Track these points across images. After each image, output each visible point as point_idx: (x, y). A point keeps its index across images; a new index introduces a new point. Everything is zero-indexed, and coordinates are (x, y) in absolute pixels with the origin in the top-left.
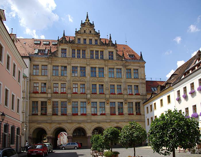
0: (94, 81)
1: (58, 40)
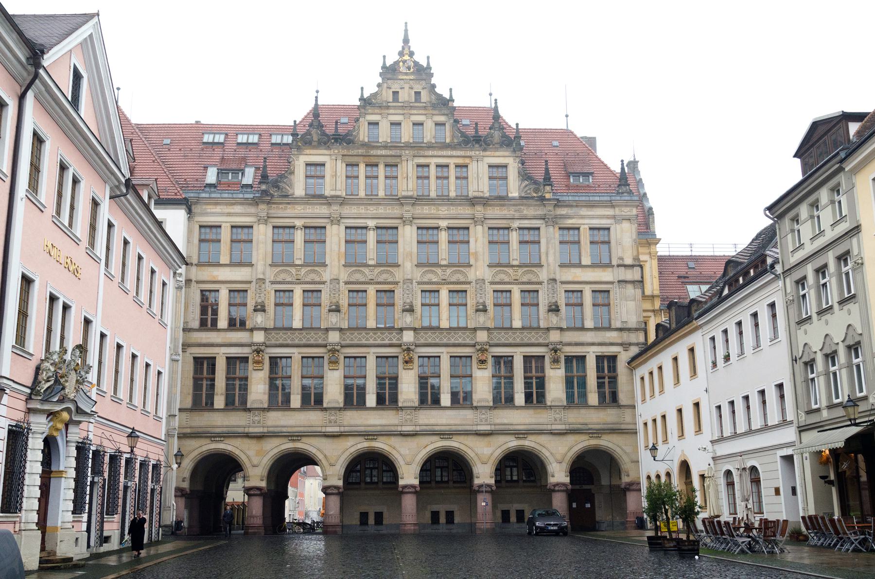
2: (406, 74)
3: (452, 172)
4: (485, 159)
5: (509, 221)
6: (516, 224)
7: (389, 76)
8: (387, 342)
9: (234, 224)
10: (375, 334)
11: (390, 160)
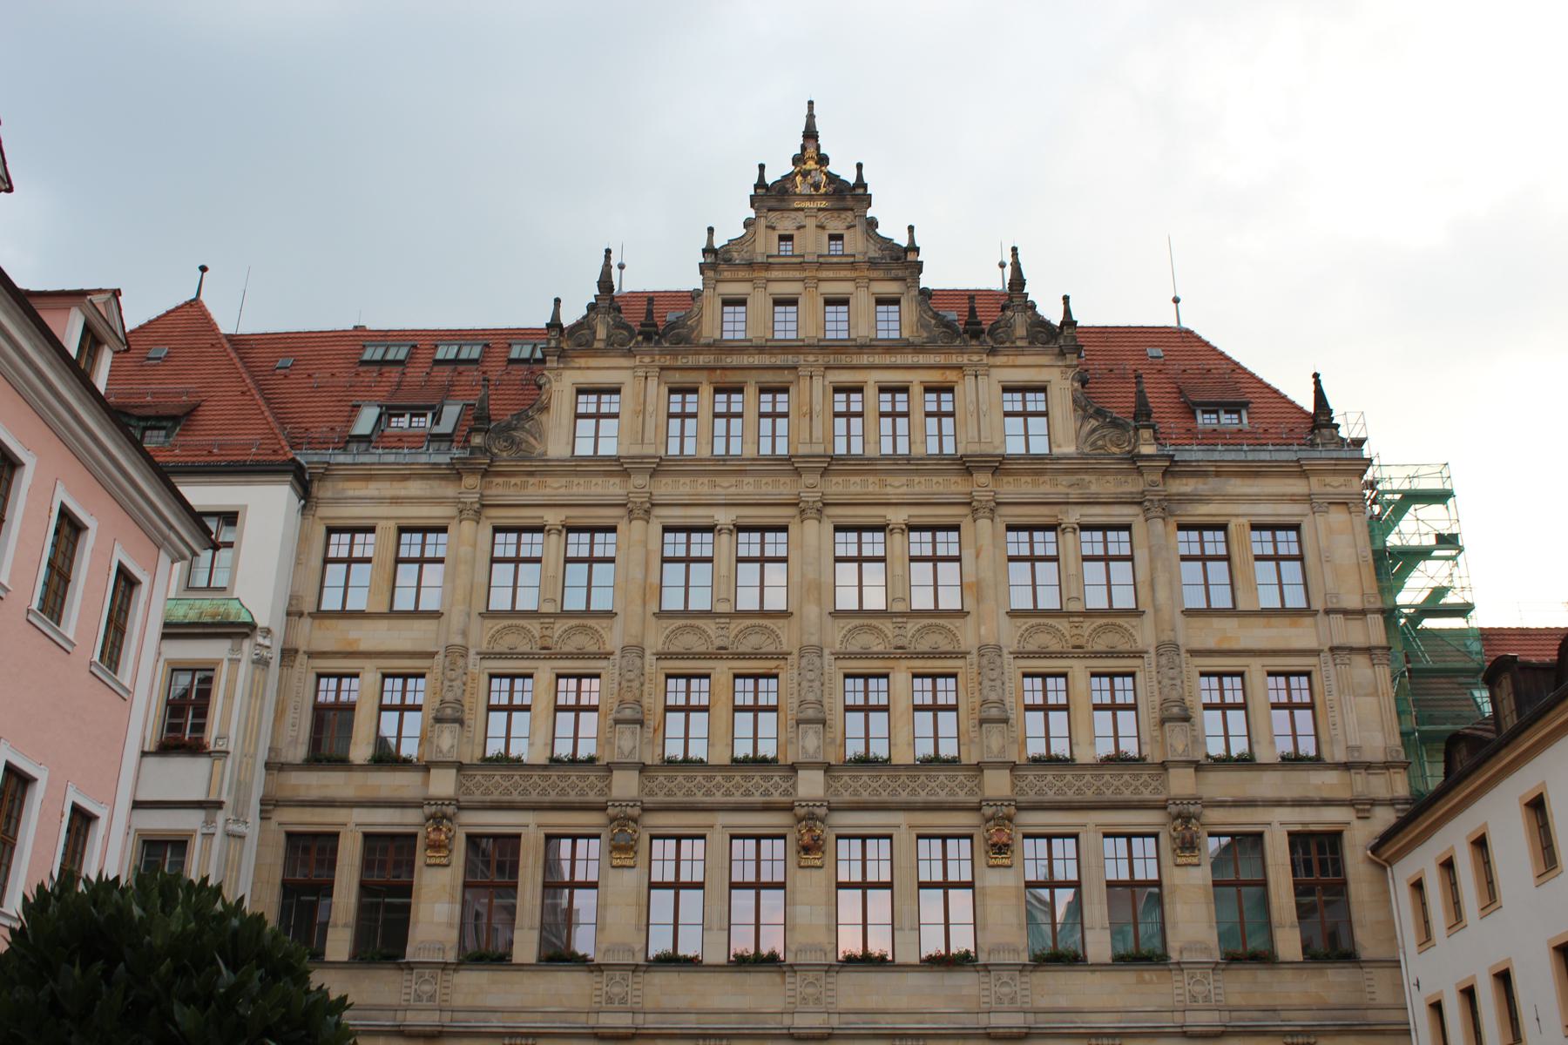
0: (866, 655)
1: (555, 324)
4: (993, 371)
5: (1056, 509)
6: (1073, 516)
7: (773, 203)
8: (757, 798)
9: (405, 523)
10: (728, 779)
11: (770, 378)
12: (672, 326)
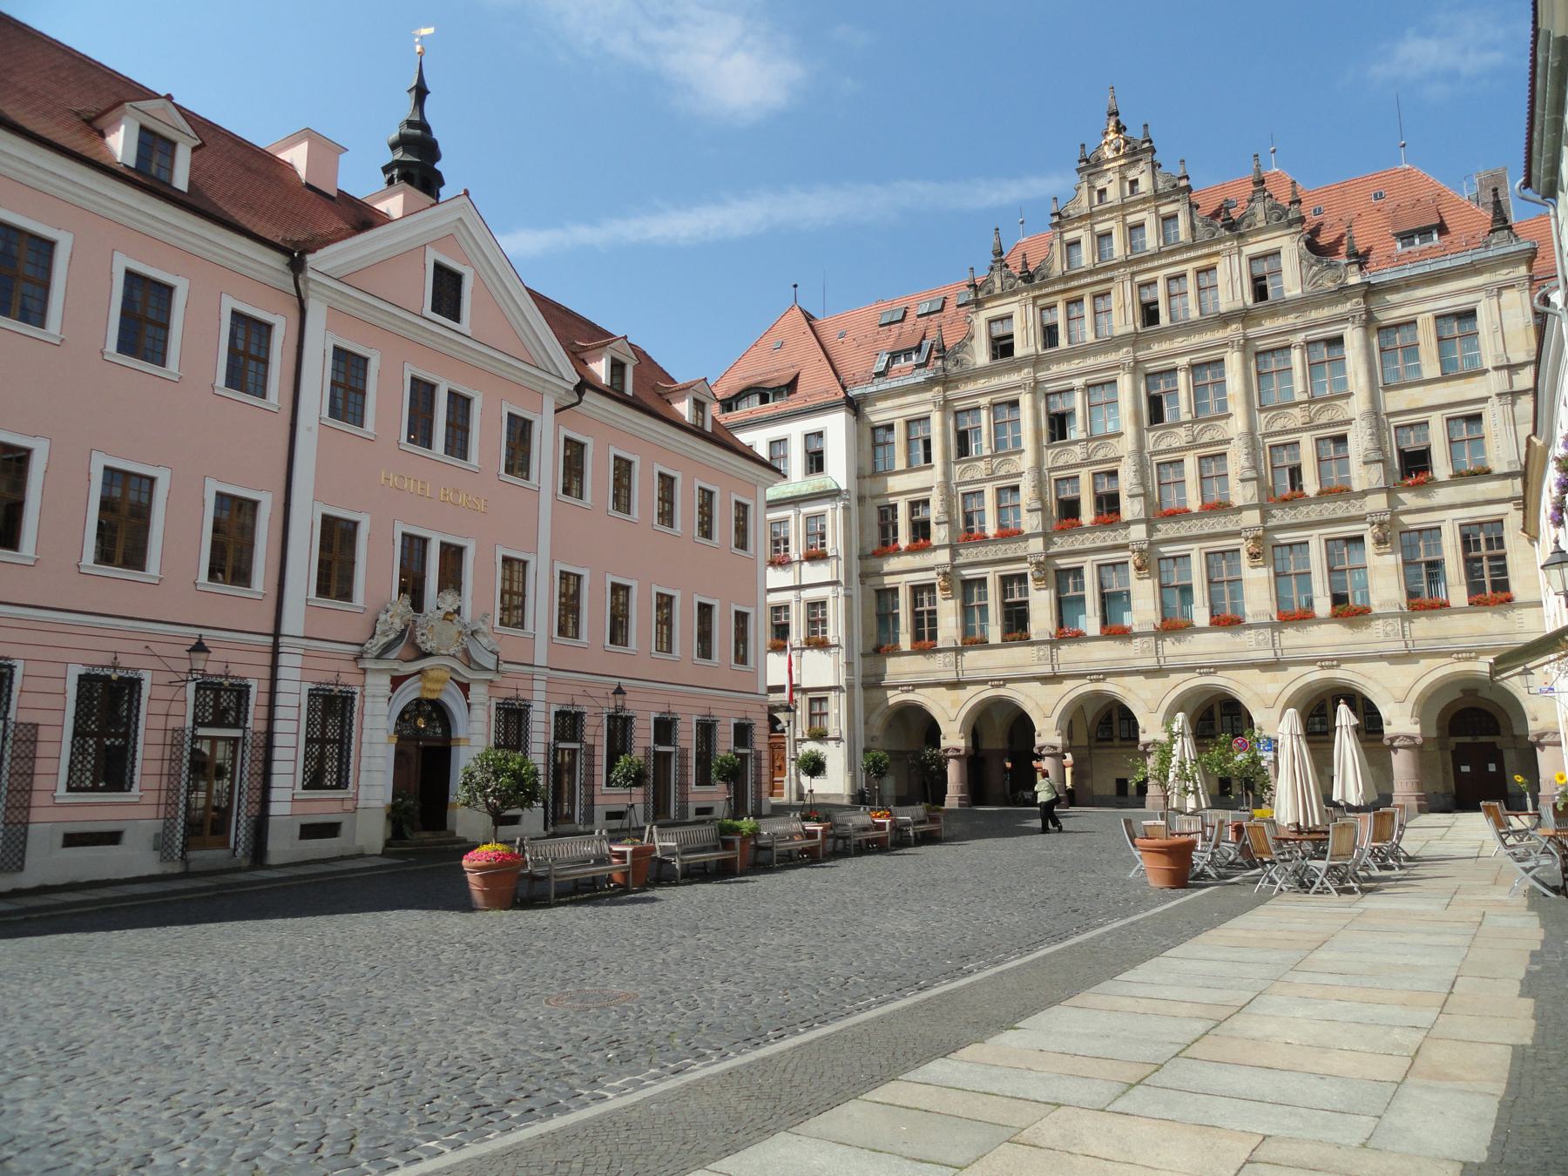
2: (1114, 159)
3: (1190, 284)
6: (1299, 338)
12: (1038, 269)
